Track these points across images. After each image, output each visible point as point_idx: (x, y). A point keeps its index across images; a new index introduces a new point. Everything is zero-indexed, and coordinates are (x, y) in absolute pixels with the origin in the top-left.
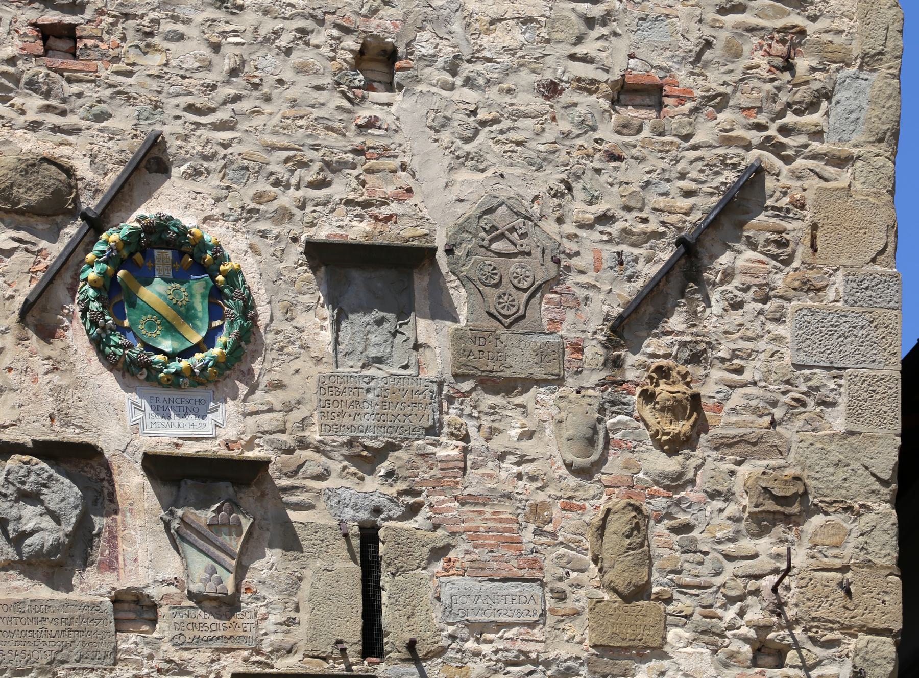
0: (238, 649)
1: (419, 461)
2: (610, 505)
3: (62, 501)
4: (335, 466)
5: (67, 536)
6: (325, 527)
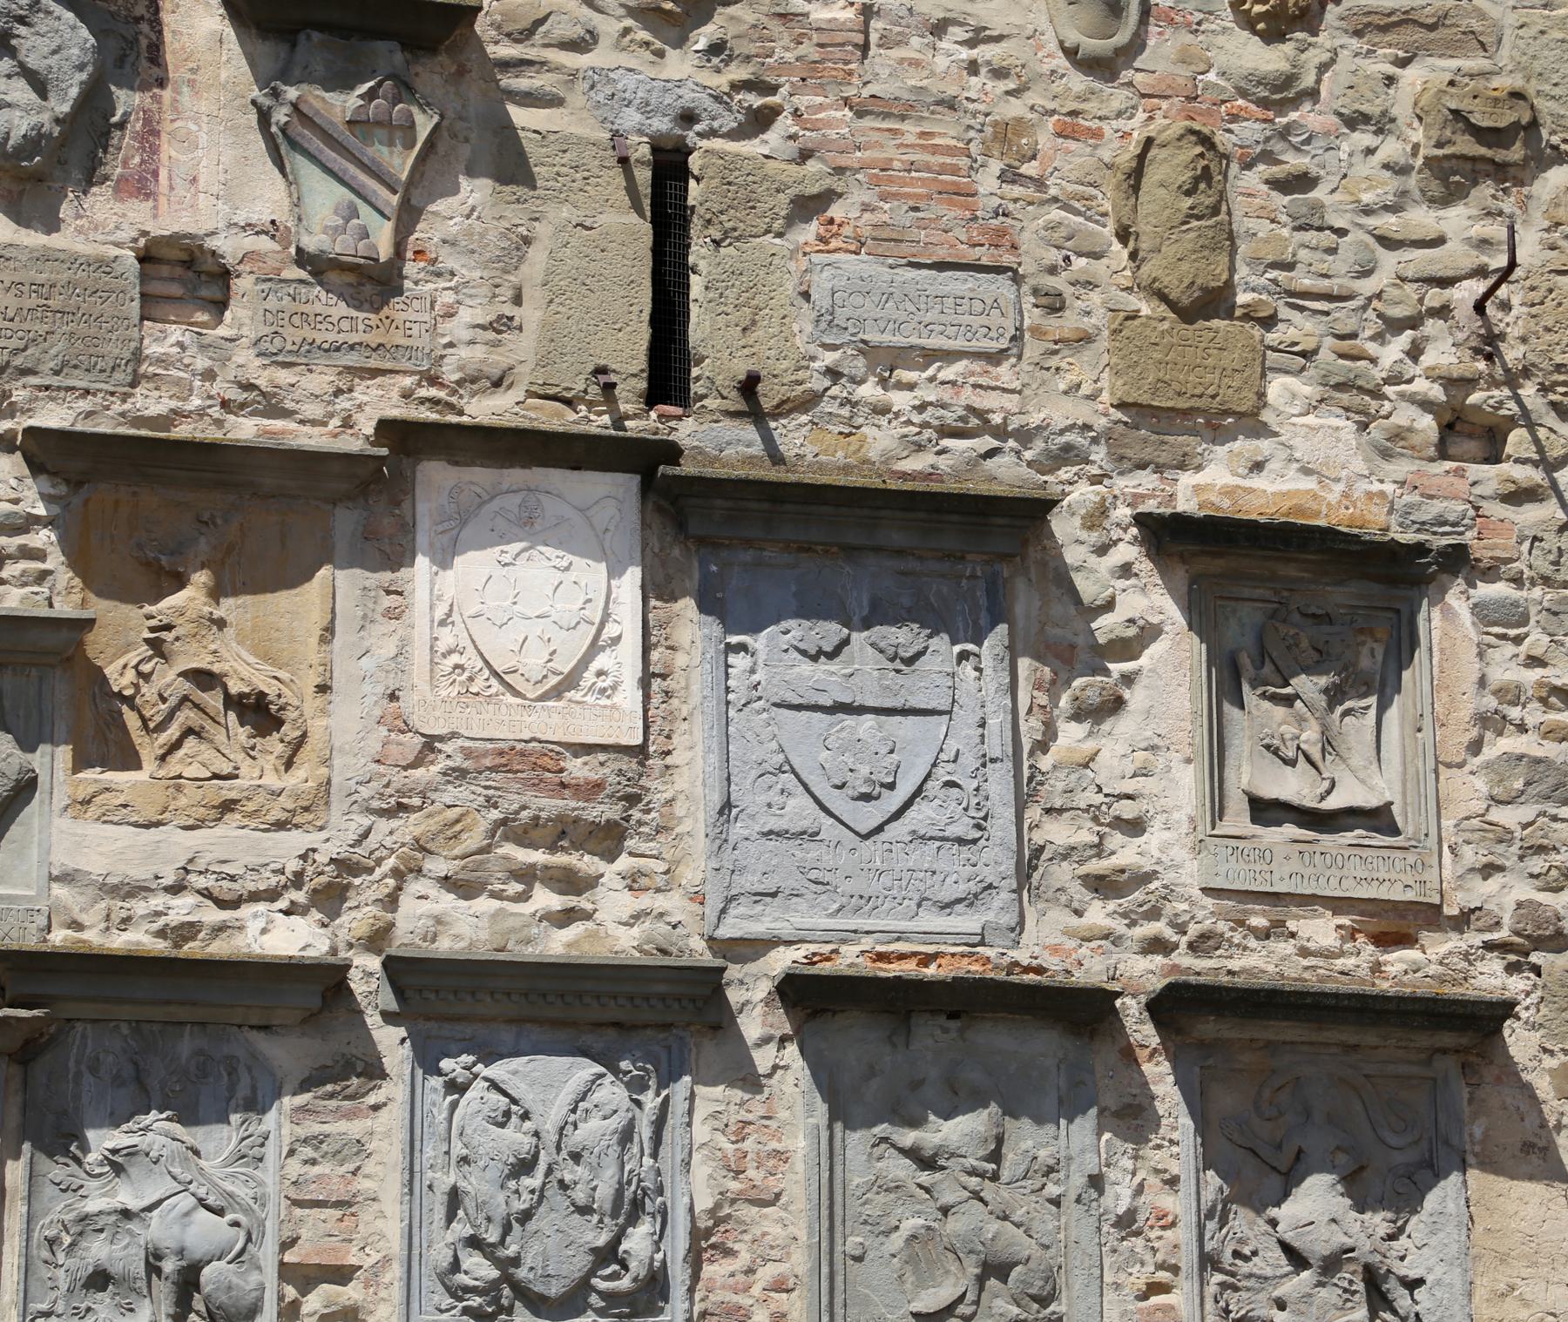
0: (391, 372)
1: (775, 27)
2: (1151, 130)
3: (54, 52)
4: (609, 27)
5: (57, 121)
6: (581, 142)
